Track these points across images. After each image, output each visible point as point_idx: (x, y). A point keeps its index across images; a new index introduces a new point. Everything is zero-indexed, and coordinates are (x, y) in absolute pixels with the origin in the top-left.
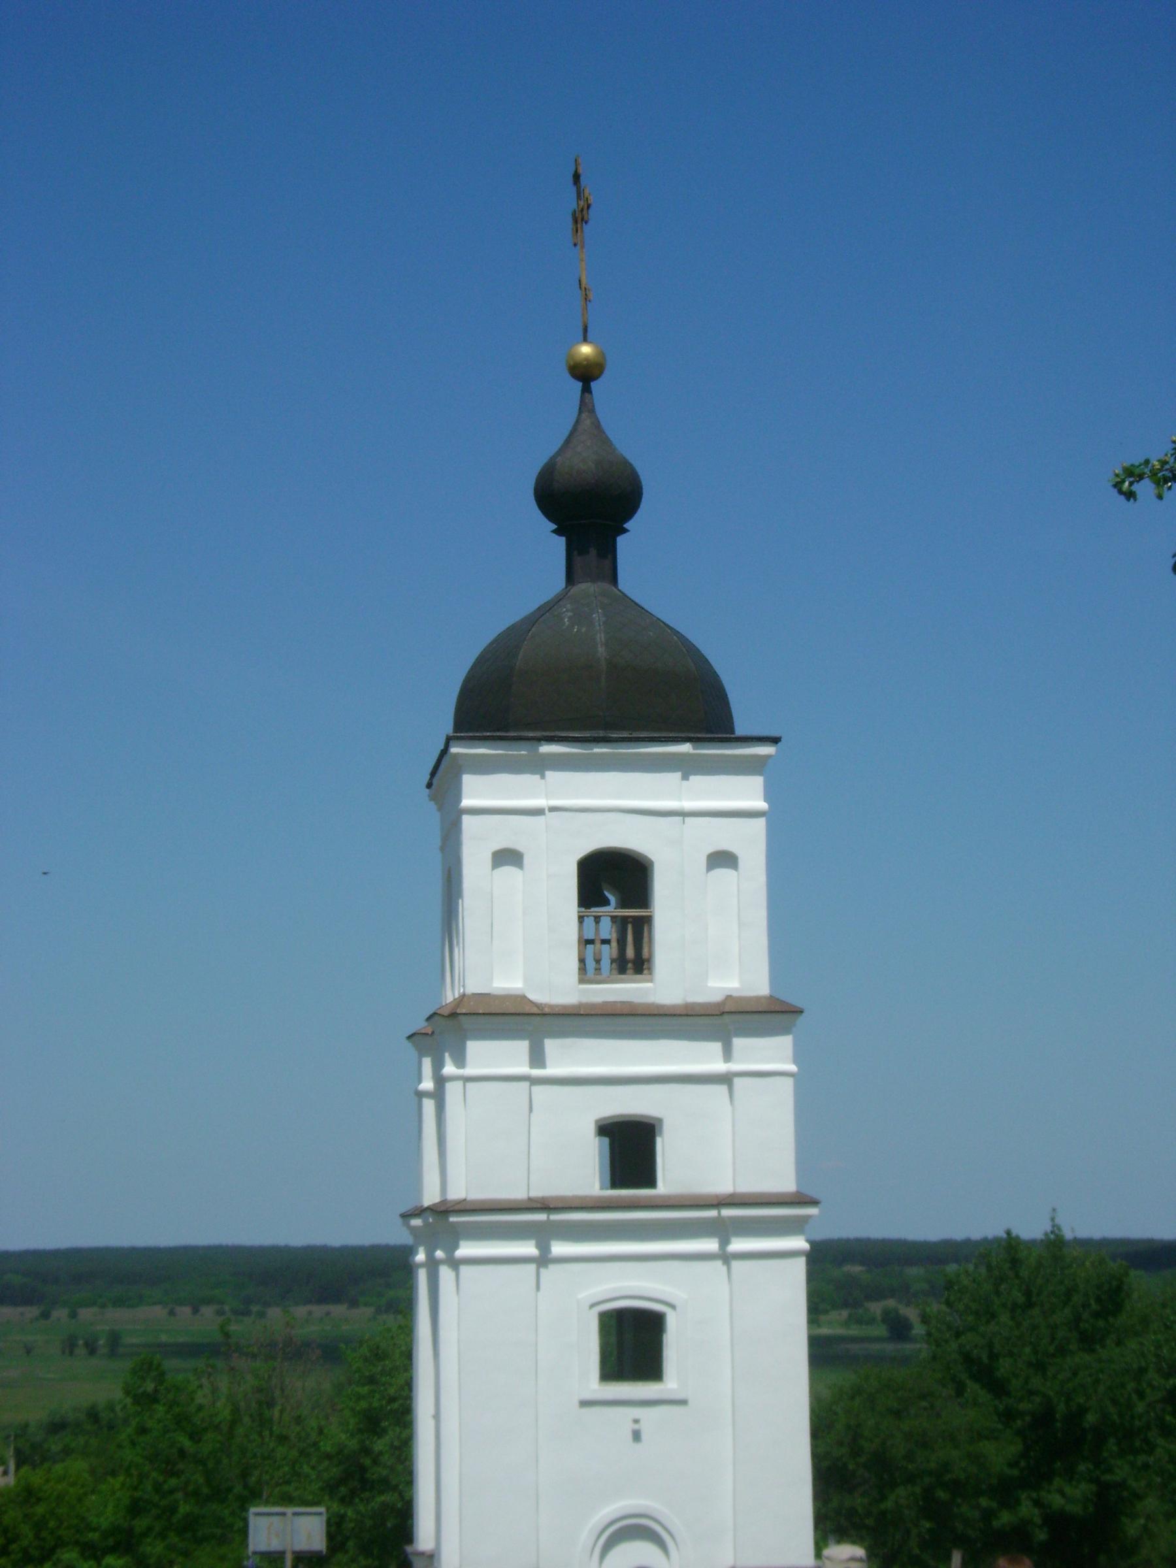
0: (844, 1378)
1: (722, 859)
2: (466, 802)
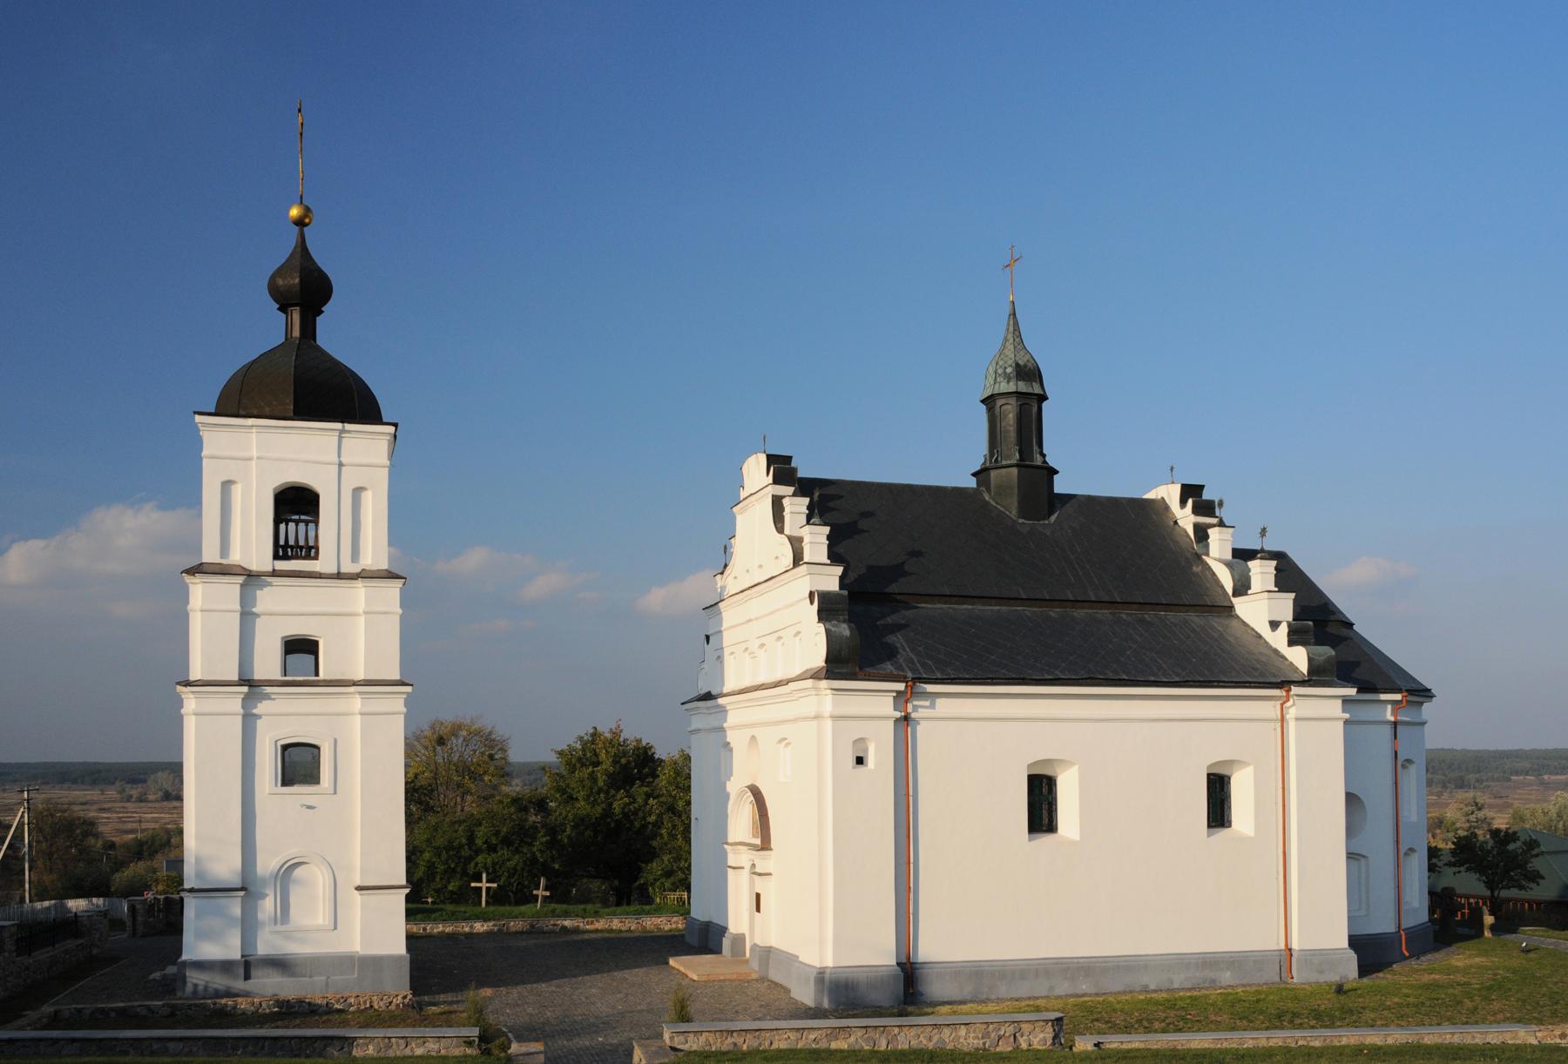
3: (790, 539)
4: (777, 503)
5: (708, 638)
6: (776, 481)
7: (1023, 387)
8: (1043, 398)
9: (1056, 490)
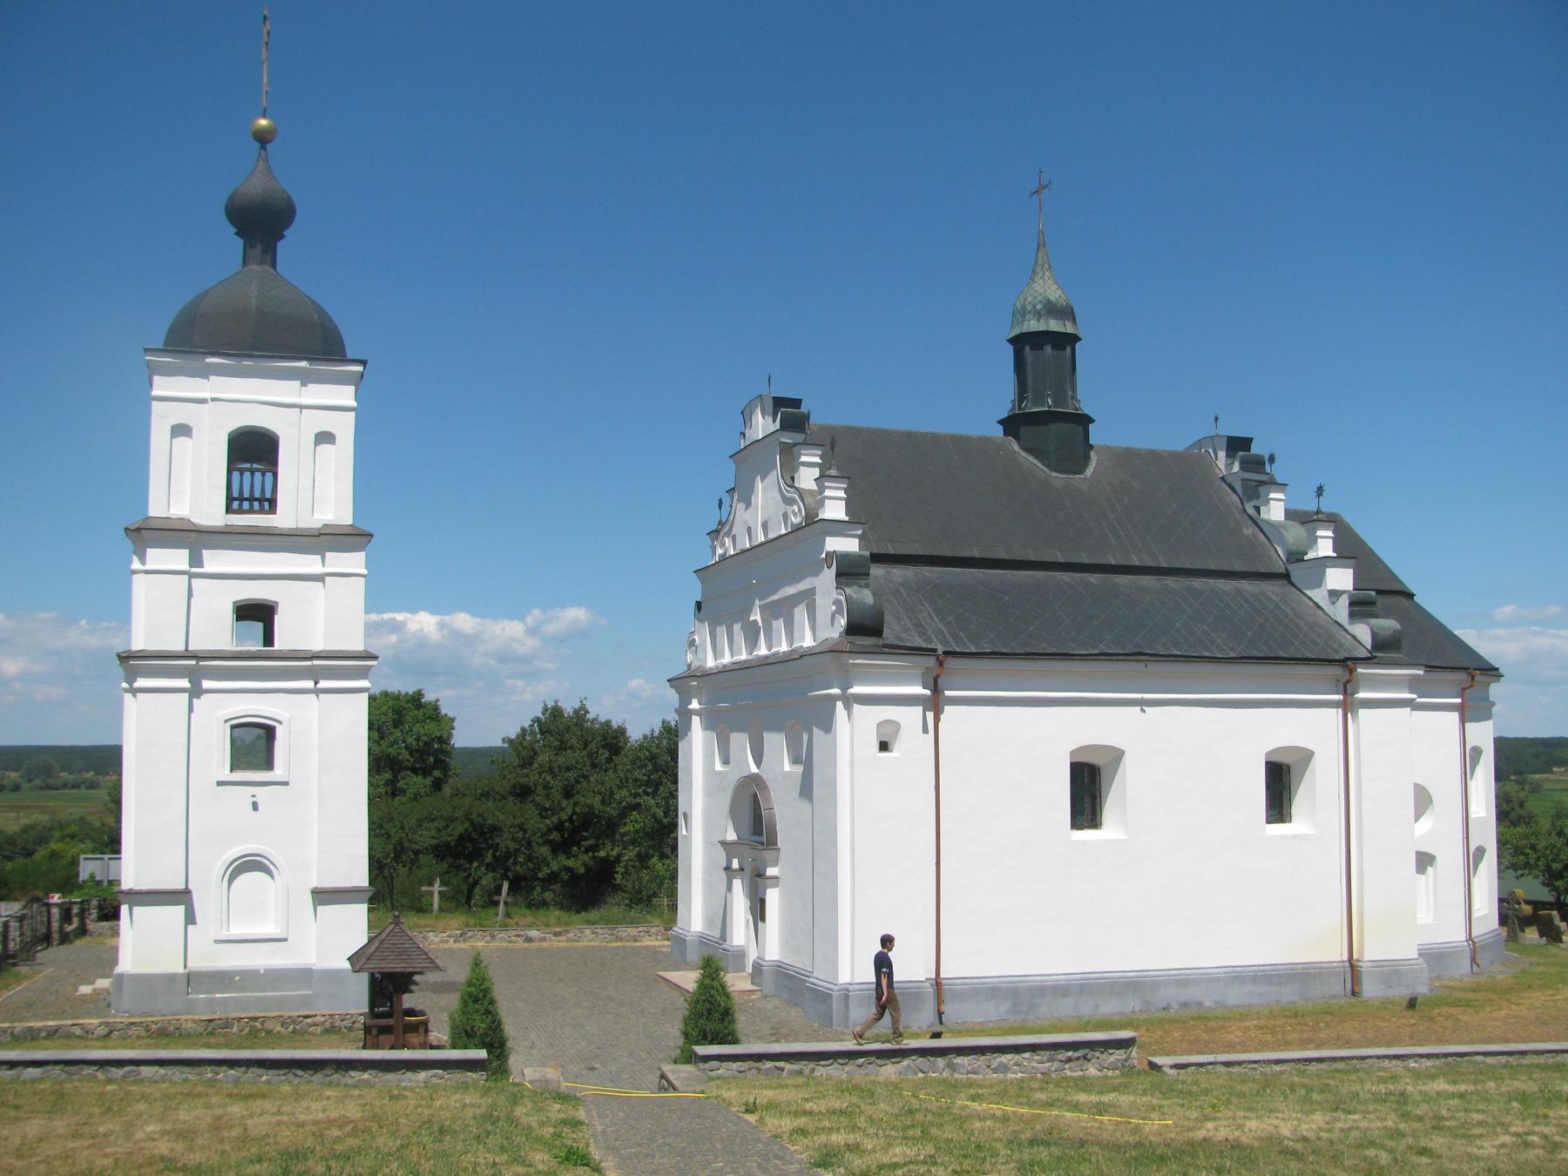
1: (325, 438)
2: (155, 393)
7: (1054, 325)
8: (1074, 339)
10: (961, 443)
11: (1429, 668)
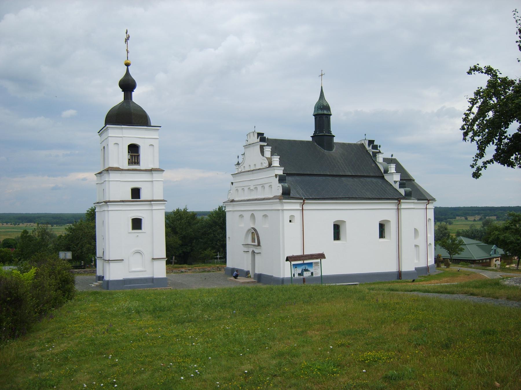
0: (169, 229)
3: (267, 158)
4: (262, 147)
5: (232, 183)
6: (261, 141)
7: (325, 112)
8: (331, 115)
9: (335, 141)
10: (302, 142)
11: (418, 199)
